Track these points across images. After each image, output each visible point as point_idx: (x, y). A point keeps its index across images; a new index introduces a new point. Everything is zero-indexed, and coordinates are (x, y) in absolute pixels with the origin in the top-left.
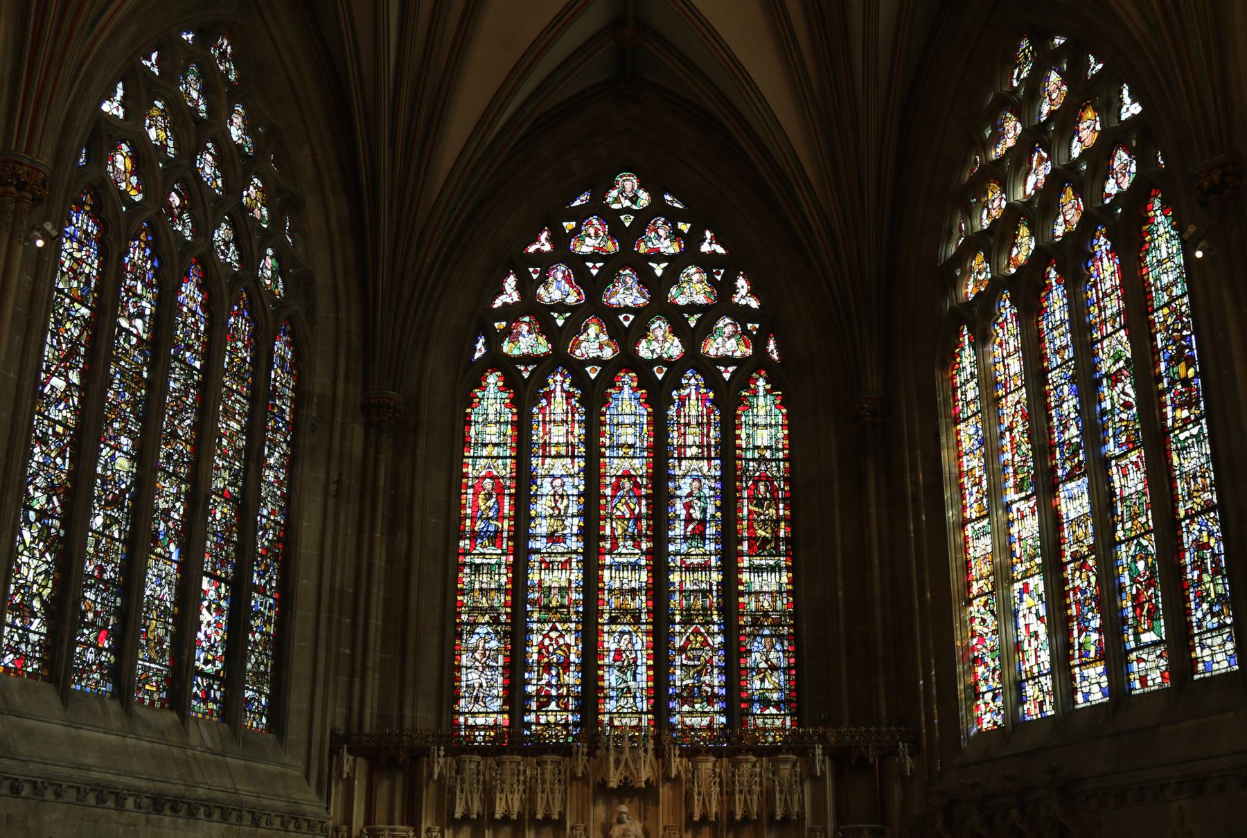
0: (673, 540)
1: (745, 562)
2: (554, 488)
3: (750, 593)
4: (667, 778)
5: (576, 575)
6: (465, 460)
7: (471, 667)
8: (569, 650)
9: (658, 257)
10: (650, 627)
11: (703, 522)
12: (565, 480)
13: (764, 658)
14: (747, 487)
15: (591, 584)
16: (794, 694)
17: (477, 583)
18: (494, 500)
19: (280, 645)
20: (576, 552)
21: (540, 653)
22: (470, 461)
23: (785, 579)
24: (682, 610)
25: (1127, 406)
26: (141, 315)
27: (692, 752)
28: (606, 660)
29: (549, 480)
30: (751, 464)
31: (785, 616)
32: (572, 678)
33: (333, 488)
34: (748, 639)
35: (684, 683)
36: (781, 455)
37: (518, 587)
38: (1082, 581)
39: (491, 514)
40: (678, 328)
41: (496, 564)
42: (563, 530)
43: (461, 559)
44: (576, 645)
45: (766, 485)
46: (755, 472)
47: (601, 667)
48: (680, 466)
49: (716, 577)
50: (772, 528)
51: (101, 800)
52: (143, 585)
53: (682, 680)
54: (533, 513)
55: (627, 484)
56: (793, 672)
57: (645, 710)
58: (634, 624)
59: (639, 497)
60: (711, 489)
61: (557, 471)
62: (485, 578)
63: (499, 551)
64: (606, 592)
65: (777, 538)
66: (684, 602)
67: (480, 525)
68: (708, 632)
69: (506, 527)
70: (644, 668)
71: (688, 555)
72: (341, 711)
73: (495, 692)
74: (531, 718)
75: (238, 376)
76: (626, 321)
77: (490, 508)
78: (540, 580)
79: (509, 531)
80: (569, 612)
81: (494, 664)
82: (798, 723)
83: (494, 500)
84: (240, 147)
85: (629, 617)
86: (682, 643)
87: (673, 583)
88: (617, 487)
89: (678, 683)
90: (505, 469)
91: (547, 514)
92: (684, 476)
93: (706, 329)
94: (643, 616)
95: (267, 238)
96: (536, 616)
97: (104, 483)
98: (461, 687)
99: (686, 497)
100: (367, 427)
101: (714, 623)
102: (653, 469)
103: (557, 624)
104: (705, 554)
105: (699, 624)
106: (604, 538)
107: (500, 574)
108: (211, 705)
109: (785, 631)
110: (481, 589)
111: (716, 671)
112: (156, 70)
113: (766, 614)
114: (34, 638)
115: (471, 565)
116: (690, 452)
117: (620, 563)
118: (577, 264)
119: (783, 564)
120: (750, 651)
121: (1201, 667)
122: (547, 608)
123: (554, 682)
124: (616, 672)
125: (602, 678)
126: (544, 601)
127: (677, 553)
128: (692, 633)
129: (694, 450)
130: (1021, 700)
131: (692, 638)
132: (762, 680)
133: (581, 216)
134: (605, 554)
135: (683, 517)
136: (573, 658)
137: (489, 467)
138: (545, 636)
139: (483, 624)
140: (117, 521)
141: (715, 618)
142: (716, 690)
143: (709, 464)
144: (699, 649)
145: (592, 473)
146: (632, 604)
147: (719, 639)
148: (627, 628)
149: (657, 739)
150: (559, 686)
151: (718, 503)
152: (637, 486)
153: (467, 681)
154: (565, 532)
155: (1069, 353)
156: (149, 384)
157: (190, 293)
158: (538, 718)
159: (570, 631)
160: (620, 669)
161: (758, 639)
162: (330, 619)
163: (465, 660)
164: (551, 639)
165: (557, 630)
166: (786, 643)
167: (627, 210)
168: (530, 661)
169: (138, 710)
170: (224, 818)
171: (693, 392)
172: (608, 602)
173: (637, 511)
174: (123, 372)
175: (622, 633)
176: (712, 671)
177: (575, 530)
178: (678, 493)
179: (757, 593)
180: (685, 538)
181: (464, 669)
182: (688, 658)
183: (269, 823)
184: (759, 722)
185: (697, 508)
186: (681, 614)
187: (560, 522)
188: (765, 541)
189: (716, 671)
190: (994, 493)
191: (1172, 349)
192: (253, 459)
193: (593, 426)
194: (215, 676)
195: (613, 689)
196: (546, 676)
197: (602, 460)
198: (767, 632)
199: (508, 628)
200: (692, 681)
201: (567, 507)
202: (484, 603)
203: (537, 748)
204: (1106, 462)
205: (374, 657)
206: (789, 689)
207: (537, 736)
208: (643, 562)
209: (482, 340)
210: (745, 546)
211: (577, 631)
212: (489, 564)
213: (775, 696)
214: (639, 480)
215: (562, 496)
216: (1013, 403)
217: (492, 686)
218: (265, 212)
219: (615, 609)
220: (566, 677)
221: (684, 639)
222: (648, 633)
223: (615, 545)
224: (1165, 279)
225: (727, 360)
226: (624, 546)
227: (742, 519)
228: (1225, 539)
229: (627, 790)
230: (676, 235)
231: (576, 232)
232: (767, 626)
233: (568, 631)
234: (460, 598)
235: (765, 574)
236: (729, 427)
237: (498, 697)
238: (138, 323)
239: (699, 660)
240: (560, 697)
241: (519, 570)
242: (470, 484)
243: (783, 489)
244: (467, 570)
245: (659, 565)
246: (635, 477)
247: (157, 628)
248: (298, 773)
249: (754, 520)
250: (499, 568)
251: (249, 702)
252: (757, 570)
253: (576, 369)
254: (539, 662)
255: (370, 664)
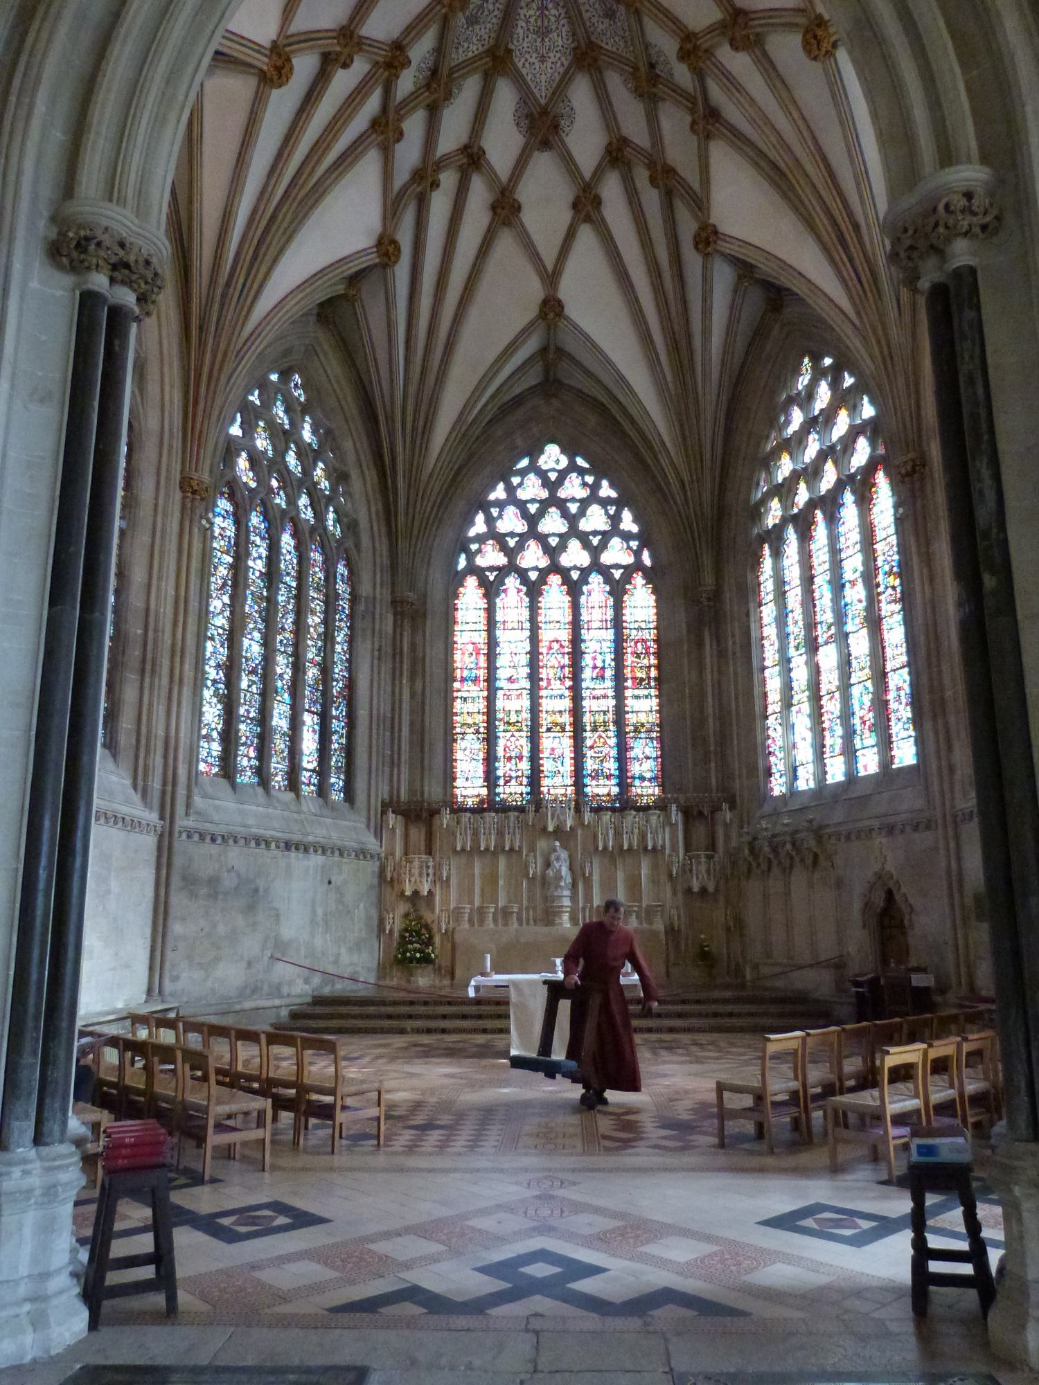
4: (583, 824)
5: (526, 703)
9: (573, 500)
11: (603, 668)
15: (535, 710)
19: (349, 751)
25: (860, 601)
26: (260, 557)
27: (598, 810)
32: (525, 766)
33: (376, 653)
36: (651, 626)
37: (490, 712)
38: (832, 707)
40: (586, 545)
43: (455, 694)
49: (612, 702)
51: (258, 844)
52: (271, 717)
55: (555, 646)
59: (564, 654)
65: (649, 678)
67: (466, 674)
72: (386, 788)
74: (499, 790)
75: (318, 590)
76: (553, 541)
82: (663, 791)
84: (310, 445)
88: (550, 648)
90: (481, 638)
93: (604, 545)
95: (329, 500)
97: (247, 660)
100: (395, 614)
106: (542, 679)
108: (312, 788)
109: (654, 735)
112: (258, 402)
113: (643, 725)
114: (215, 754)
116: (594, 625)
118: (521, 505)
121: (896, 761)
122: (509, 723)
126: (506, 719)
129: (598, 624)
130: (795, 778)
133: (523, 473)
135: (591, 665)
140: (254, 682)
145: (534, 639)
149: (577, 802)
152: (562, 646)
155: (827, 566)
156: (268, 600)
157: (287, 541)
162: (378, 734)
163: (459, 755)
167: (553, 470)
169: (273, 792)
170: (324, 853)
171: (596, 590)
174: (253, 593)
183: (349, 855)
184: (639, 791)
188: (642, 680)
190: (783, 650)
191: (887, 568)
192: (328, 638)
193: (534, 609)
194: (313, 771)
196: (508, 765)
198: (643, 735)
202: (470, 721)
203: (504, 808)
204: (847, 635)
205: (405, 756)
207: (504, 800)
209: (463, 556)
213: (648, 775)
216: (794, 597)
218: (327, 483)
224: (884, 524)
225: (617, 566)
228: (911, 685)
229: (559, 833)
230: (585, 484)
231: (520, 485)
236: (618, 608)
238: (259, 562)
240: (517, 777)
241: (490, 700)
245: (577, 698)
247: (280, 744)
248: (363, 826)
251: (333, 785)
252: (637, 697)
253: (522, 574)
255: (403, 760)
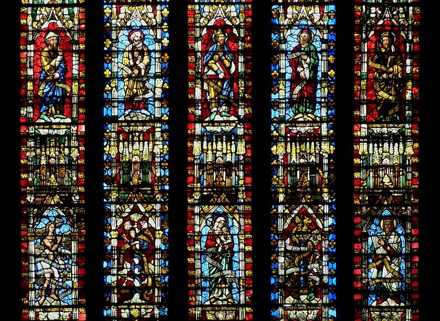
0: (276, 105)
1: (363, 130)
2: (131, 42)
3: (367, 168)
6: (23, 10)
7: (40, 256)
8: (154, 234)
10: (248, 208)
11: (313, 82)
12: (145, 32)
13: (383, 243)
14: (367, 39)
16: (415, 284)
17: (43, 158)
18: (59, 58)
20: (159, 120)
21: (119, 238)
22: (29, 10)
23: (410, 150)
24: (286, 187)
28: (198, 246)
29: (126, 32)
30: (373, 9)
31: (409, 194)
34: (364, 221)
35: (288, 272)
39: (57, 75)
41: (66, 135)
42: (144, 93)
44: (162, 229)
45: (390, 37)
46: (377, 19)
47: (192, 254)
48: (285, 13)
49: (327, 148)
50: (396, 89)
53: (286, 269)
54: (107, 73)
56: (417, 259)
57: (242, 301)
58: (230, 205)
59: (236, 53)
60: (323, 41)
61: (136, 22)
62: (53, 152)
63: (69, 120)
64: (196, 167)
66: (289, 178)
67: (44, 89)
68: (316, 213)
69: (75, 90)
70: (241, 255)
71: (294, 122)
73: (69, 283)
77: (55, 68)
78: (118, 154)
79: (79, 96)
80: (153, 191)
81: (67, 252)
83: (59, 58)
85: (223, 196)
86: (286, 226)
87: (277, 157)
88: (208, 41)
89: (281, 272)
91: (125, 74)
92: (290, 26)
94: (240, 196)
96: (114, 196)
98: (30, 278)
99: (293, 52)
101: (324, 203)
102: (252, 18)
103: (139, 205)
104: (314, 121)
105: (306, 203)
106: (193, 103)
107: (70, 147)
110: (48, 165)
111: (325, 258)
113: (386, 191)
115: (36, 137)
117: (212, 133)
119: (408, 132)
120: (367, 235)
123: (136, 271)
124: (208, 259)
125: (193, 267)
127: (282, 120)
128: (297, 215)
131: (298, 220)
132: (380, 269)
134: (195, 122)
135: (288, 76)
136: (158, 243)
137: (53, 18)
138: (125, 219)
139: (53, 206)
141: (326, 197)
142: (325, 279)
143: (321, 11)
144: (306, 233)
146: (228, 181)
147: (330, 221)
148: (221, 209)
150: (142, 277)
151: (331, 58)
153: (36, 271)
154: (147, 96)
158: (119, 311)
159: (154, 213)
160: (215, 256)
161: (376, 221)
163: (32, 247)
164: (133, 223)
165: (139, 212)
166: (409, 225)
168: (109, 248)
172: (199, 180)
173: (233, 70)
175: (216, 215)
176: (321, 258)
177: (159, 93)
178: (283, 46)
179: (376, 168)
180: (291, 103)
181: (33, 258)
182: (293, 243)
185: (306, 66)
186: (285, 193)
187: (140, 85)
189: (325, 258)
195: (205, 279)
197: (189, 7)
199: (82, 210)
200: (298, 269)
201: (148, 66)
206: (411, 278)
208: (240, 131)
210: (364, 111)
211: (162, 213)
212: (57, 135)
214: (235, 31)
215: (142, 53)
217: (65, 276)
219: (207, 187)
220: (151, 267)
221: (289, 221)
222: (245, 215)
223: (207, 112)
226: (218, 112)
227: (361, 78)
232: (387, 206)
233: (152, 213)
234: (24, 176)
235: (386, 145)
237: (72, 289)
239: (306, 246)
242: (30, 38)
243: (411, 42)
244: (32, 144)
246: (231, 28)
249: (375, 79)
250: (69, 140)
254: (119, 248)
